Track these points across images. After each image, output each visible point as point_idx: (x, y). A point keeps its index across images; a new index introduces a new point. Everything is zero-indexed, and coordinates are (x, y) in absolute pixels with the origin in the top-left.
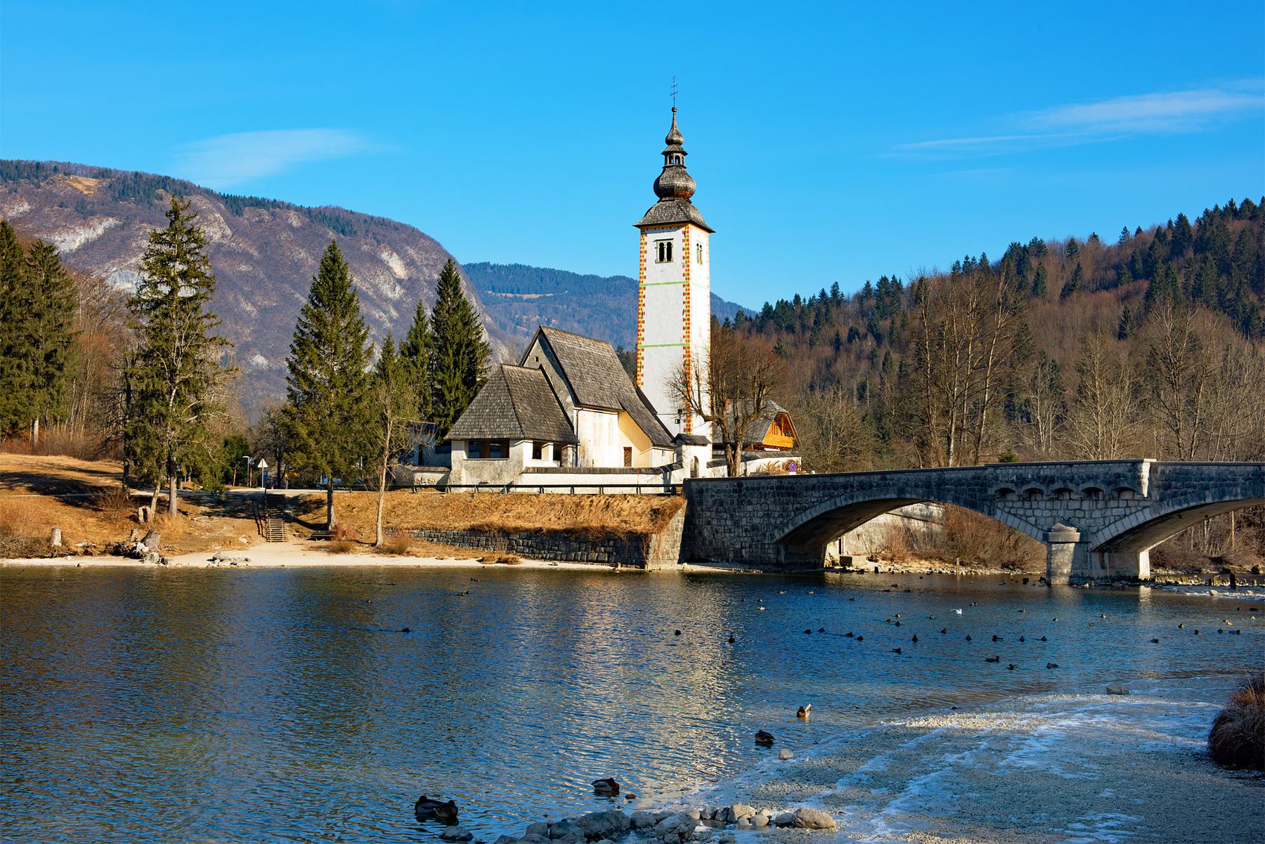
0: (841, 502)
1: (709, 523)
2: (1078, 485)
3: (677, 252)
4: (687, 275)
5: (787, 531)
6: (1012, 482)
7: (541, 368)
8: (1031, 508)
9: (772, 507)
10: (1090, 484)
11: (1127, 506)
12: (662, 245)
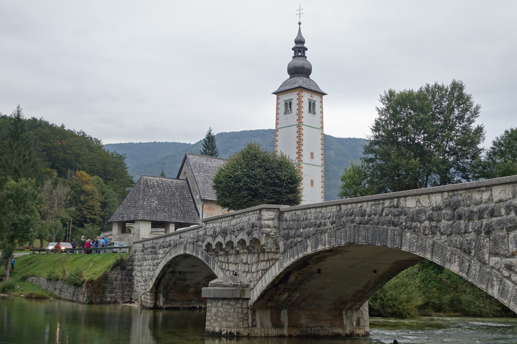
1: (136, 276)
2: (236, 237)
3: (295, 107)
4: (299, 120)
7: (187, 180)
8: (228, 263)
10: (240, 237)
11: (268, 260)
12: (286, 103)
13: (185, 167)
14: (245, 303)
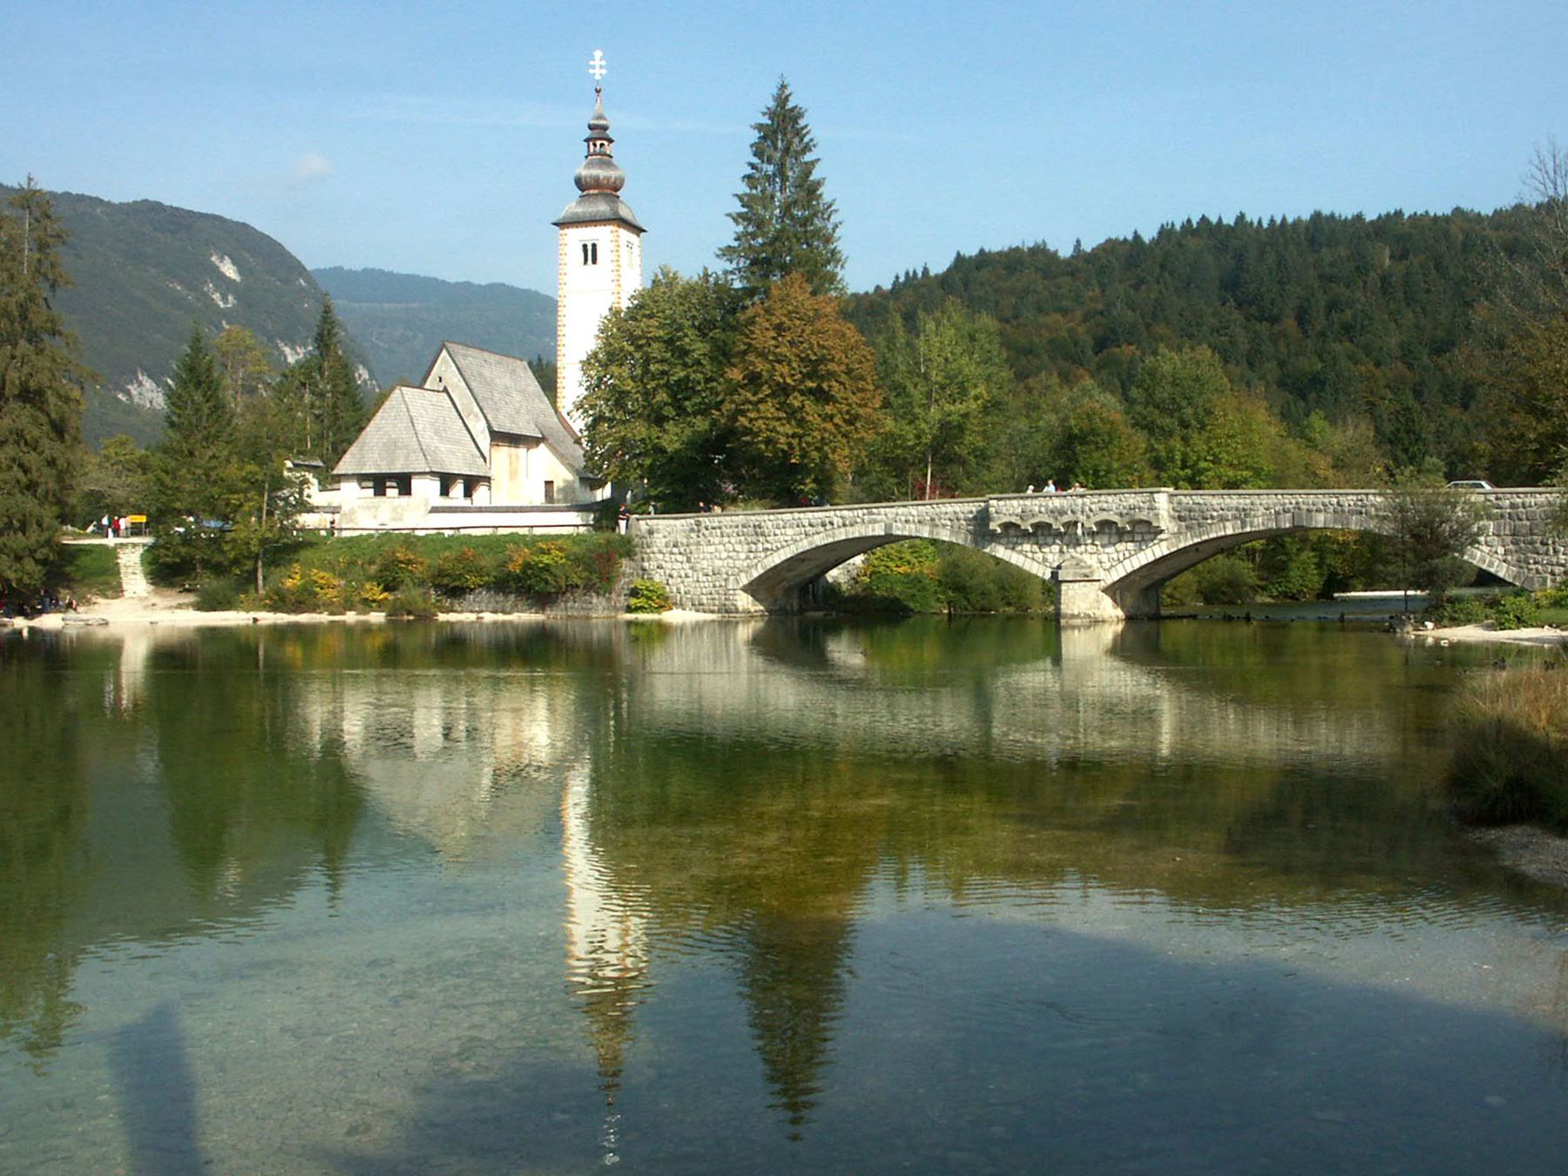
0: (820, 540)
5: (755, 574)
6: (1017, 515)
7: (445, 390)
9: (738, 548)
12: (585, 246)
13: (441, 367)
14: (1097, 583)
